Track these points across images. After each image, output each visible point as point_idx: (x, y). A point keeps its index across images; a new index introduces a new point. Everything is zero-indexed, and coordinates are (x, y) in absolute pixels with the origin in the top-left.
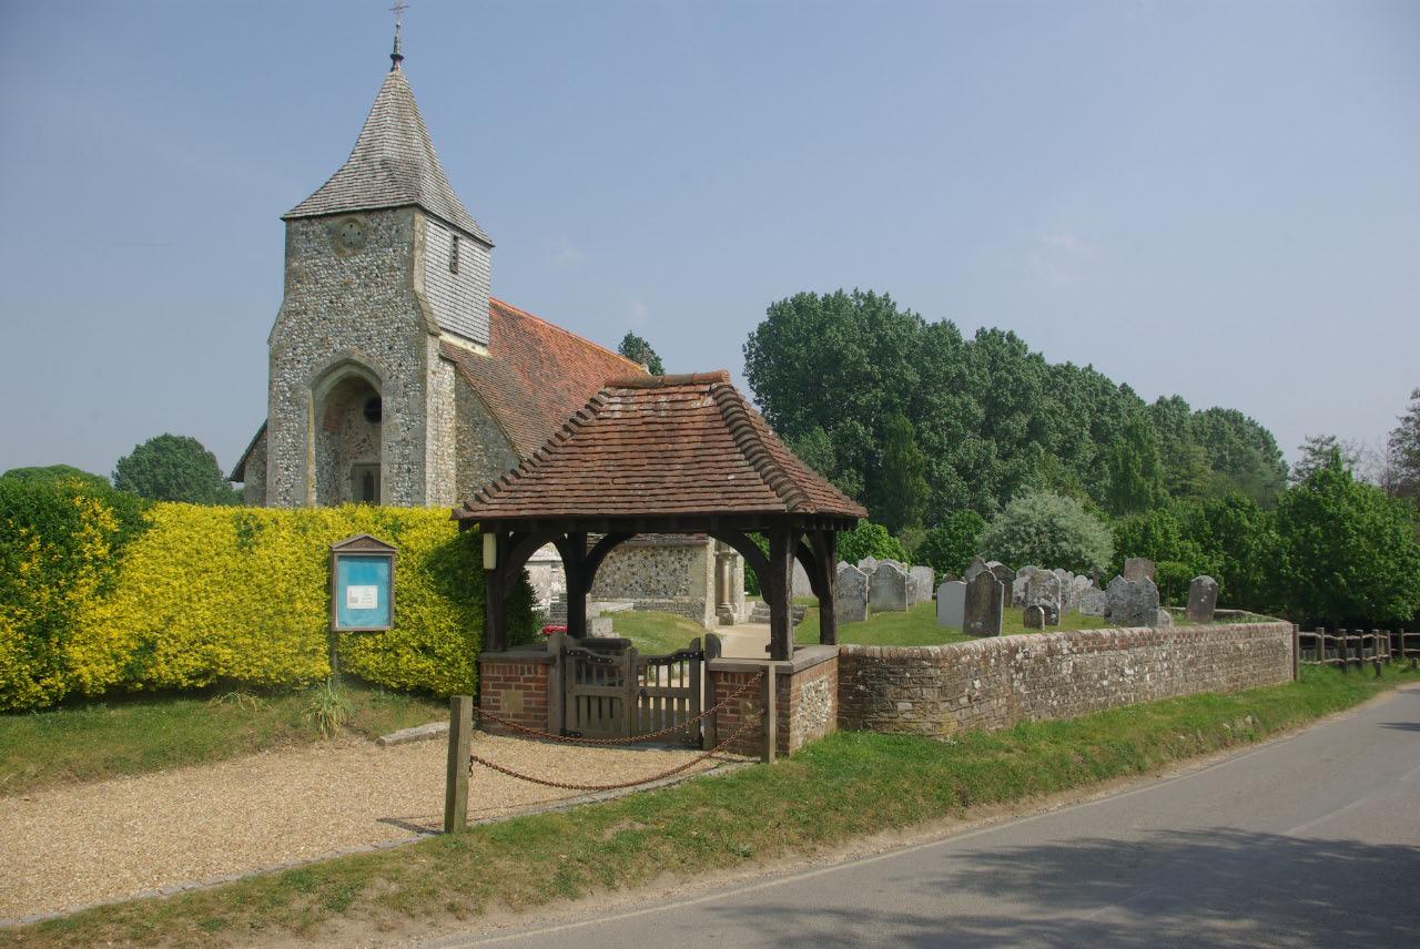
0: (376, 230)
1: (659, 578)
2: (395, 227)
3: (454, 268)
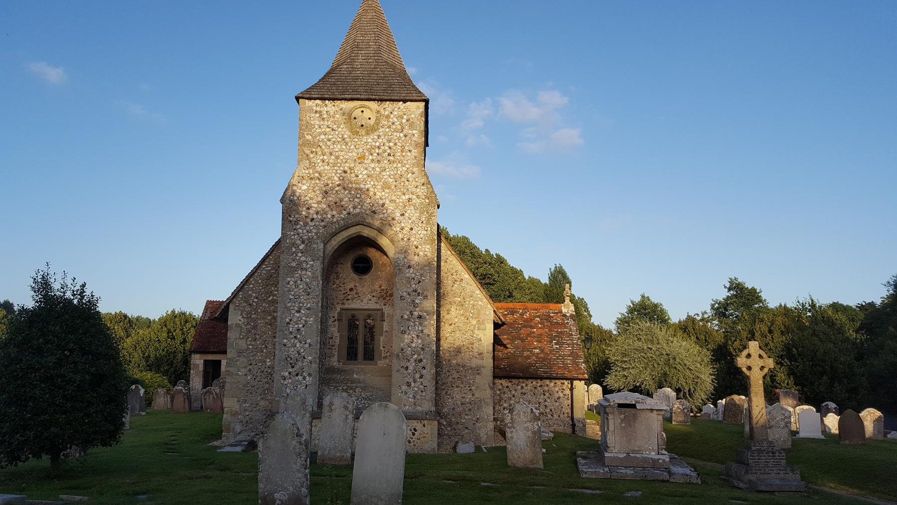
0: (388, 117)
1: (547, 403)
2: (405, 117)
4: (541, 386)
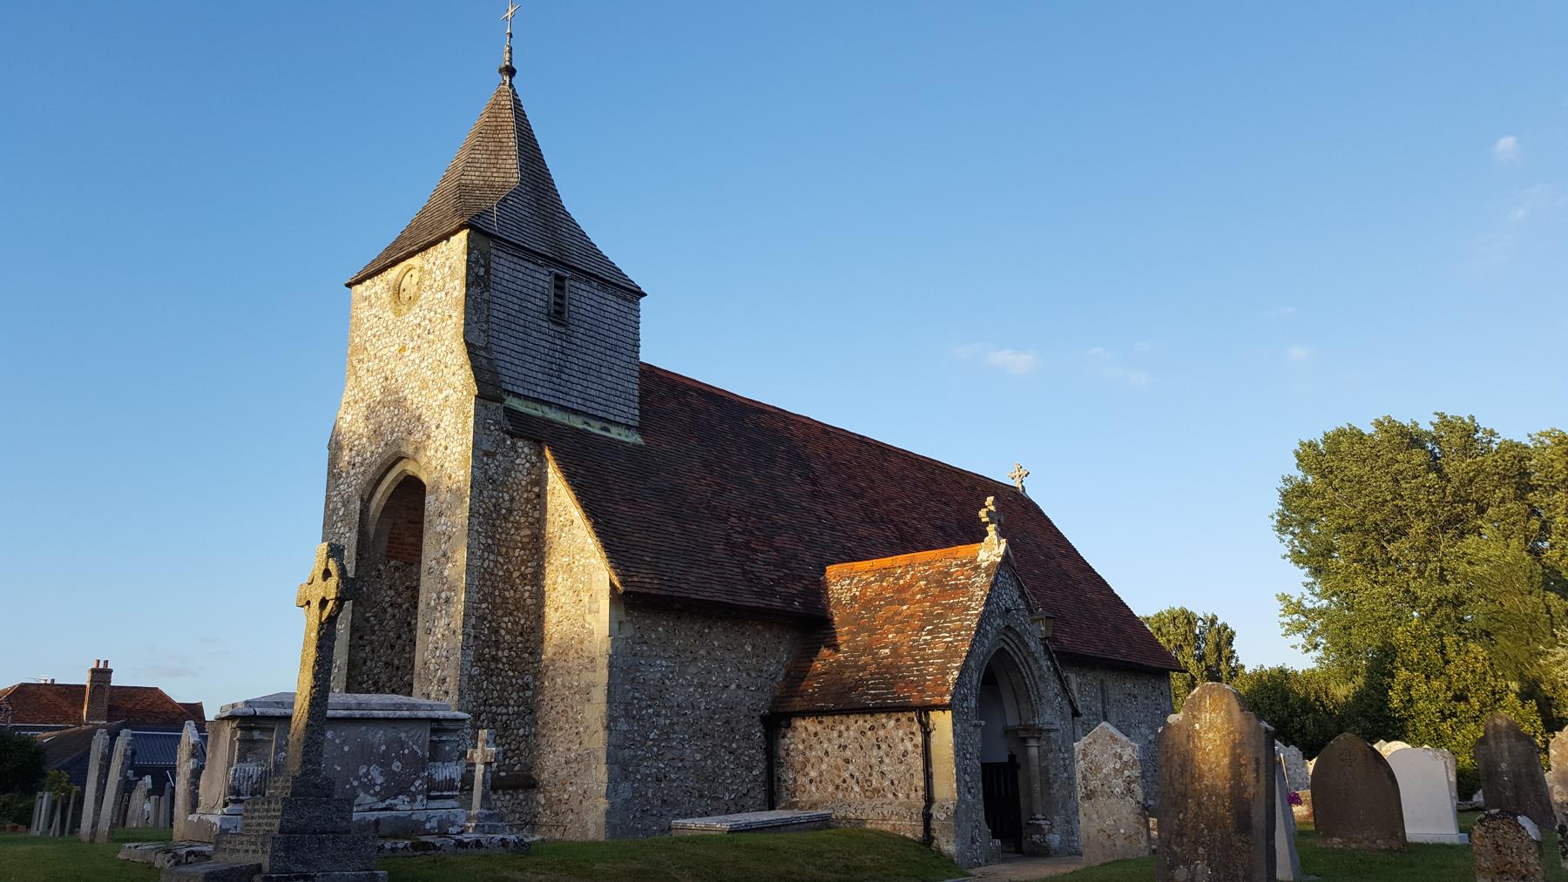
3: (558, 314)
4: (872, 728)
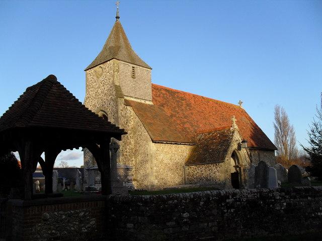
3: (133, 77)
